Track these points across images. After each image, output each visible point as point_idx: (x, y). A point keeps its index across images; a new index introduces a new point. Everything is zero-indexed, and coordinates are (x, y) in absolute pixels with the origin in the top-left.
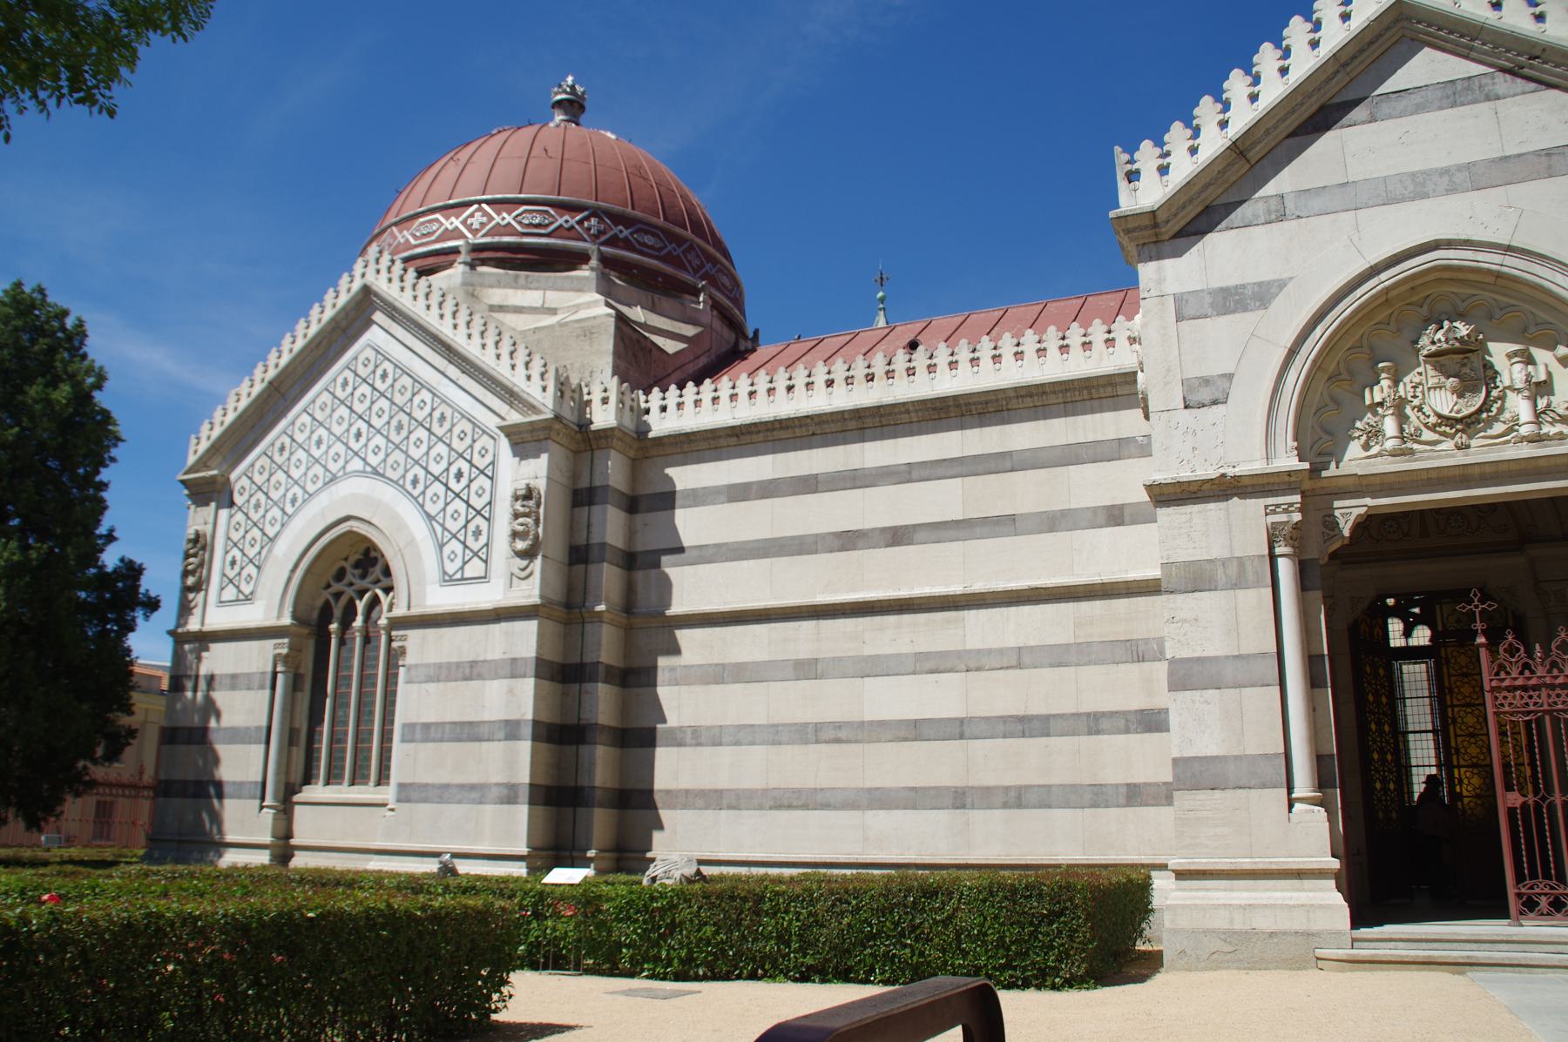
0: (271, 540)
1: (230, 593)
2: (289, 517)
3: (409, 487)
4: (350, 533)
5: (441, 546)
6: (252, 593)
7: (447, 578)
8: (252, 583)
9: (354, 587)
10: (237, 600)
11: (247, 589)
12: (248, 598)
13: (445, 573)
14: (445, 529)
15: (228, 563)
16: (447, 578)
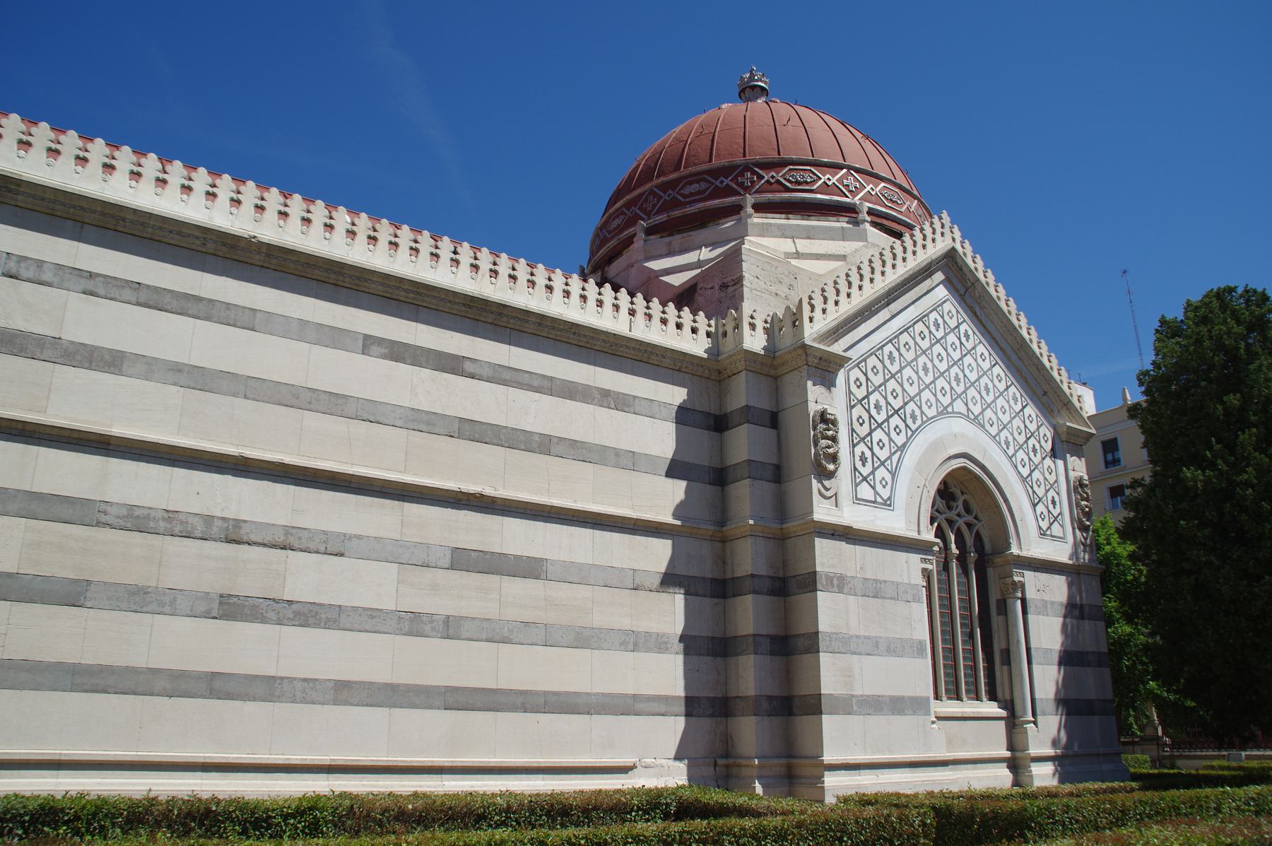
0: (902, 448)
1: (865, 491)
2: (913, 432)
3: (1005, 447)
4: (965, 467)
5: (1034, 505)
6: (889, 498)
7: (1042, 532)
8: (889, 487)
9: (944, 516)
10: (874, 502)
11: (885, 493)
12: (888, 503)
13: (1040, 528)
14: (1034, 492)
15: (857, 458)
16: (1042, 532)
